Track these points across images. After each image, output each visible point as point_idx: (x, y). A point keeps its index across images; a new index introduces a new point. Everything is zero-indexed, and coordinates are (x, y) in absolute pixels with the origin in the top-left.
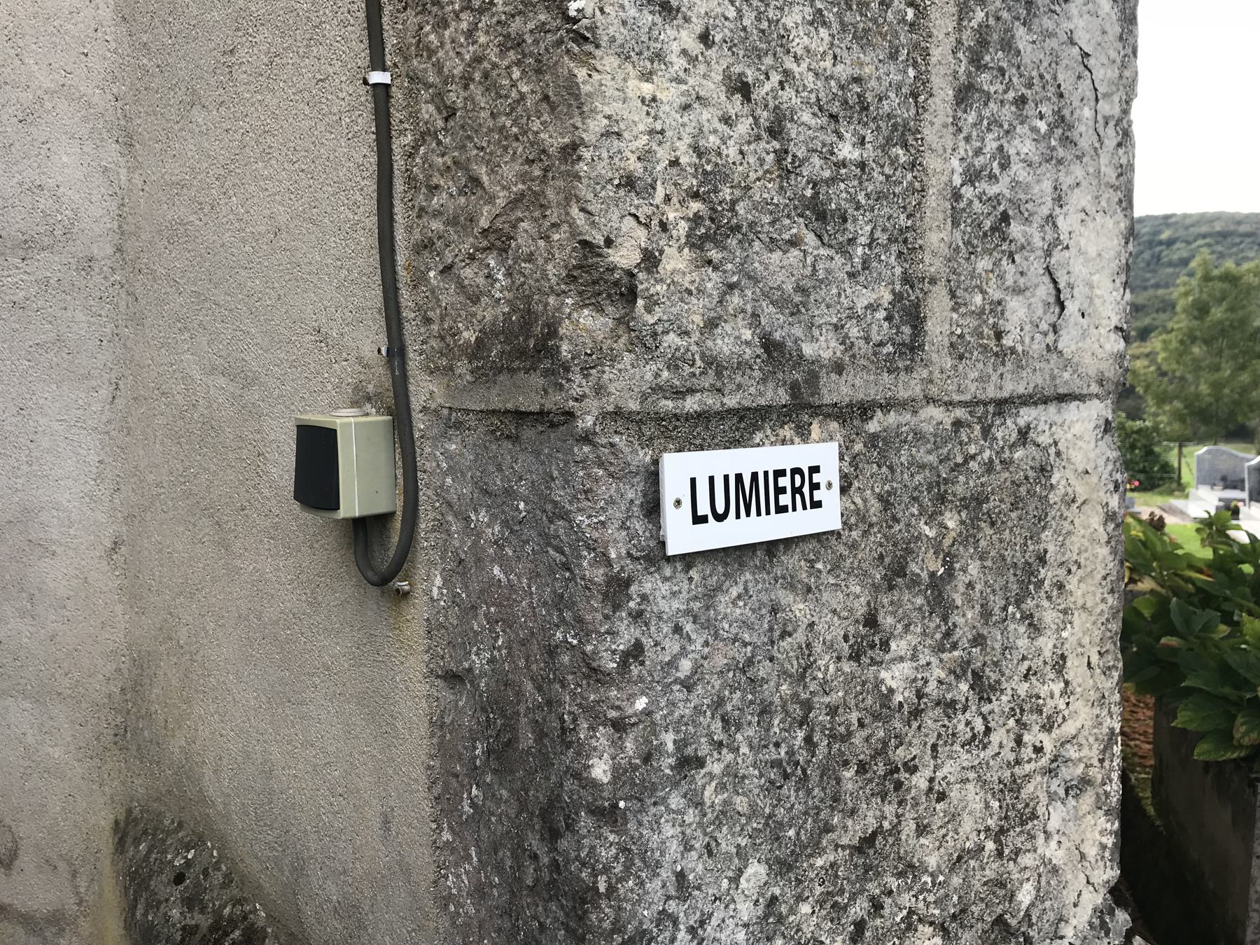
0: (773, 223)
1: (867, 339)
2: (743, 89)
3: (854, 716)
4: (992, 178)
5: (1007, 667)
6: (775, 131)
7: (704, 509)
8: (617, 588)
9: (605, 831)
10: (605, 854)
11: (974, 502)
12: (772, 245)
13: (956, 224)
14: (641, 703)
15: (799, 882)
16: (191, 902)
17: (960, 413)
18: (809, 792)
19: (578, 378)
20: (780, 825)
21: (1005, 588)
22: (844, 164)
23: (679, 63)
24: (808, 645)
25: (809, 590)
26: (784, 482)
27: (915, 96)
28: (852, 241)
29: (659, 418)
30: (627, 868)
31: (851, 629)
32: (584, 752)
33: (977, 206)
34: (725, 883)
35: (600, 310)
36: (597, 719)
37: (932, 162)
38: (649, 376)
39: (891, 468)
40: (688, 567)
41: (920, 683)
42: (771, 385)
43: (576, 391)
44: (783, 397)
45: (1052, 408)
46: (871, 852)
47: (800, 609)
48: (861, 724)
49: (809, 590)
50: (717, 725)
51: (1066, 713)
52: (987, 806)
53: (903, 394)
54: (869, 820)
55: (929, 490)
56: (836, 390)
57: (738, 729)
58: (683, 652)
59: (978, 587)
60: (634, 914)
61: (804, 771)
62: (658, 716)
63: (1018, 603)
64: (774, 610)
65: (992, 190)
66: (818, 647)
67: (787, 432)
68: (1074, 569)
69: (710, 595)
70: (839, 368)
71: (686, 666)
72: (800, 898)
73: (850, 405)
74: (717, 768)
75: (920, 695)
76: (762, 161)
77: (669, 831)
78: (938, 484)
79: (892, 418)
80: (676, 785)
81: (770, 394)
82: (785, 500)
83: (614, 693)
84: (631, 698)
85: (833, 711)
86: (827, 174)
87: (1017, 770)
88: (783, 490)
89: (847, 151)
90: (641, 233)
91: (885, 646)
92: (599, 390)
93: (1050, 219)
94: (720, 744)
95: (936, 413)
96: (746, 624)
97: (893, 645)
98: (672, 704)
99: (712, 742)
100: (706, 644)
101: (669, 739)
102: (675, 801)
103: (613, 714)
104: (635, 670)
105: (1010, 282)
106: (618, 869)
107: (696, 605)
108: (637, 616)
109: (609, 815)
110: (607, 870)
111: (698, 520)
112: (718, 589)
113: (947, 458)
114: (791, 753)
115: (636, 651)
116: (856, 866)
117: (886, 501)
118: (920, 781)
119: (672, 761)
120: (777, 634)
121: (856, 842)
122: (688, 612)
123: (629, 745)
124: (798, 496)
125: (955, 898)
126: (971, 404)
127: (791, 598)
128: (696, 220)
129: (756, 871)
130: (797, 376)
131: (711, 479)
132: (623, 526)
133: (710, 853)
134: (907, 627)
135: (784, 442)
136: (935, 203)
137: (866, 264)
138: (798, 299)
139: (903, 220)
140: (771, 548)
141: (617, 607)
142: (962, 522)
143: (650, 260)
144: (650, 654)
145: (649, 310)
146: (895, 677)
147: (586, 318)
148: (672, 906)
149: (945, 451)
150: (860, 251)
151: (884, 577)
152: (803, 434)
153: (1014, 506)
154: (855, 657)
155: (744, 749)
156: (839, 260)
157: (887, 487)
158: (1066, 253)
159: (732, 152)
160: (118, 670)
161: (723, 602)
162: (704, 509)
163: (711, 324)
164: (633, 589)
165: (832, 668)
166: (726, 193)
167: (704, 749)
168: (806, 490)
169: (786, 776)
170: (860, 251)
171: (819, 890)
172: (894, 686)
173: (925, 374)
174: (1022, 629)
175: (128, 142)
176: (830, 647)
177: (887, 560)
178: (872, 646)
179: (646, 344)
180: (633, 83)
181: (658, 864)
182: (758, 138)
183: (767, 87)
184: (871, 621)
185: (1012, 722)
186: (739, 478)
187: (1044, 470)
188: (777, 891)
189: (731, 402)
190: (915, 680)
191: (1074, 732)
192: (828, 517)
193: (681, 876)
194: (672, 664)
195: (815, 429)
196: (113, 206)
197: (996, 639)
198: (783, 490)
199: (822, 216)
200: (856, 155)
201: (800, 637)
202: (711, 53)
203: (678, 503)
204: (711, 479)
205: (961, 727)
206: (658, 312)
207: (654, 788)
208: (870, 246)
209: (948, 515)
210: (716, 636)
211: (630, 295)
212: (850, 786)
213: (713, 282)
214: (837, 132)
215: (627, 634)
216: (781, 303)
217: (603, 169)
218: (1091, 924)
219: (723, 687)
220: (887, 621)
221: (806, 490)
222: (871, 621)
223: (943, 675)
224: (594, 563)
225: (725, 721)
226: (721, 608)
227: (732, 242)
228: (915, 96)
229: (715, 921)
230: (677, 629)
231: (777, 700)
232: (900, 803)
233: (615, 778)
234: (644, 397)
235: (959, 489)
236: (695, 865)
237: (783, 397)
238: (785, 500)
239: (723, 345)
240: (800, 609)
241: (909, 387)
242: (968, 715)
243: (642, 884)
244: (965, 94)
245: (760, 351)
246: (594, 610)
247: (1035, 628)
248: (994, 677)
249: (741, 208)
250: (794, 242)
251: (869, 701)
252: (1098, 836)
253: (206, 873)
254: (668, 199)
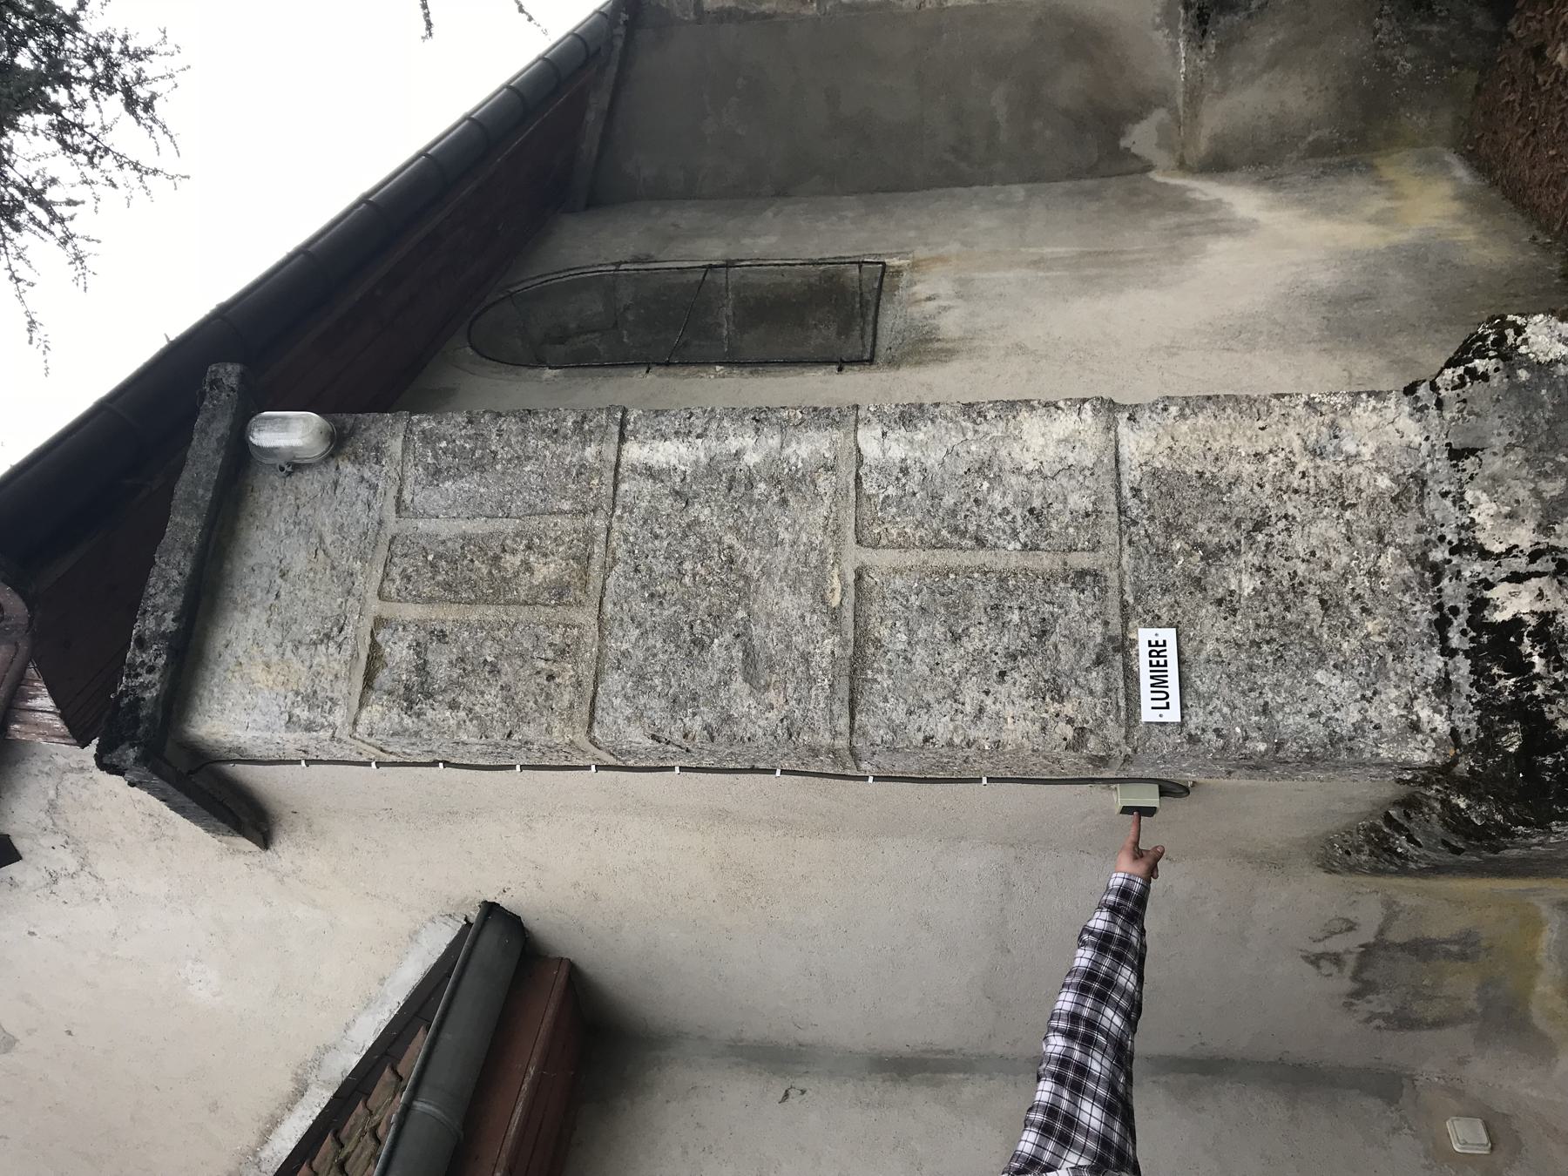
1: (1093, 604)
2: (1002, 674)
3: (1262, 614)
4: (1014, 520)
5: (1254, 502)
6: (1014, 657)
7: (1163, 704)
8: (1193, 739)
9: (1286, 747)
10: (1295, 747)
12: (1058, 659)
13: (1037, 548)
14: (1238, 730)
15: (1331, 650)
16: (1359, 851)
19: (1113, 752)
20: (1302, 660)
21: (1213, 502)
22: (1021, 619)
23: (998, 706)
24: (1226, 642)
25: (1201, 641)
26: (1154, 661)
27: (985, 573)
28: (1052, 614)
29: (1128, 718)
30: (1302, 739)
33: (1028, 531)
34: (1321, 692)
35: (1087, 740)
36: (1243, 746)
37: (1013, 565)
38: (1112, 724)
39: (1151, 586)
40: (1187, 706)
41: (1253, 570)
42: (1115, 664)
43: (1118, 753)
44: (1119, 657)
45: (1123, 468)
46: (1329, 602)
47: (1210, 647)
48: (1266, 610)
49: (1201, 641)
50: (1253, 695)
51: (1288, 450)
52: (1325, 518)
53: (1117, 584)
54: (1313, 604)
56: (1116, 629)
57: (1256, 683)
58: (1220, 711)
59: (1211, 525)
60: (1321, 739)
61: (1282, 646)
63: (1220, 492)
64: (1209, 661)
65: (1020, 521)
66: (1227, 637)
67: (1133, 653)
68: (1208, 446)
69: (1198, 695)
70: (1106, 623)
71: (1226, 710)
72: (1339, 650)
73: (1121, 617)
74: (1270, 695)
75: (1259, 569)
76: (1027, 665)
77: (1291, 721)
78: (1158, 555)
79: (1127, 588)
80: (1273, 716)
81: (1118, 664)
82: (1162, 663)
83: (1233, 740)
84: (1236, 734)
85: (1258, 626)
86: (1026, 628)
87: (1312, 492)
88: (1158, 662)
89: (1015, 617)
90: (1061, 724)
91: (1232, 593)
92: (1117, 745)
93: (1029, 475)
94: (1261, 693)
95: (1125, 558)
96: (1213, 678)
97: (1233, 588)
98: (1241, 716)
99: (1259, 697)
100: (1218, 699)
101: (1254, 719)
102: (1279, 717)
103: (1241, 741)
104: (1224, 732)
105: (1061, 506)
106: (1302, 742)
107: (1202, 704)
108: (1204, 730)
109: (1279, 746)
110: (1301, 747)
111: (1168, 707)
112: (1196, 692)
113: (1146, 548)
114: (1271, 654)
115: (1217, 731)
116: (1334, 612)
117: (1165, 591)
118: (1302, 568)
119: (1263, 718)
120: (1219, 659)
121: (1322, 612)
122: (1204, 708)
123: (1254, 735)
124: (1161, 654)
125: (1369, 542)
126: (1121, 533)
127: (1204, 652)
128: (1052, 699)
129: (1320, 676)
130: (1110, 649)
131: (1153, 699)
132: (1169, 736)
133: (1306, 699)
135: (1138, 655)
136: (1030, 561)
137: (1061, 607)
138: (1078, 645)
140: (1181, 662)
141: (1200, 741)
142: (1178, 538)
143: (1070, 721)
144: (1219, 726)
146: (1249, 585)
147: (1091, 745)
148: (1323, 719)
149: (1142, 550)
150: (1056, 610)
151: (1200, 592)
152: (1134, 643)
153: (1172, 495)
154: (1234, 611)
155: (1265, 680)
156: (1060, 621)
157: (1159, 590)
158: (1045, 463)
159: (1026, 681)
161: (1203, 689)
162: (1163, 704)
163: (1091, 693)
164: (1193, 732)
165: (1238, 627)
166: (1041, 684)
167: (1261, 701)
168: (1158, 649)
169: (1281, 657)
170: (1056, 610)
171: (1338, 638)
172: (1252, 587)
174: (1236, 492)
176: (1228, 628)
177: (1193, 589)
178: (1232, 601)
179: (1101, 724)
180: (1009, 727)
184: (1219, 602)
185: (1285, 497)
186: (1152, 685)
187: (1155, 474)
188: (1332, 663)
189: (1121, 684)
190: (1251, 573)
191: (1300, 441)
192: (1169, 635)
193: (1311, 715)
194: (1224, 716)
195: (1132, 636)
196: (989, 846)
197: (1239, 511)
198: (1158, 662)
199: (1044, 632)
200: (1016, 612)
201: (1221, 647)
202: (991, 689)
203: (1161, 716)
204: (1153, 699)
205: (1280, 538)
206: (1088, 718)
208: (1053, 604)
209: (1173, 548)
210: (1215, 693)
211: (1083, 729)
212: (1294, 616)
213: (1075, 691)
214: (1009, 623)
215: (1211, 735)
216: (1081, 654)
217: (1040, 740)
218: (1419, 421)
219: (1237, 690)
220: (1221, 592)
221: (1158, 649)
222: (1219, 602)
223: (1251, 553)
225: (1251, 690)
226: (1205, 690)
227: (1059, 681)
228: (985, 573)
230: (1211, 713)
231: (1247, 661)
232: (1310, 582)
233: (1266, 742)
234: (1120, 726)
235: (1160, 540)
236: (1310, 707)
237: (1119, 657)
238: (1162, 663)
239: (1099, 687)
241: (1113, 575)
242: (1275, 533)
243: (1310, 734)
244: (980, 542)
245: (1101, 666)
246: (1200, 748)
247: (1237, 480)
248: (1259, 512)
249: (1046, 677)
250: (1056, 647)
251: (1256, 603)
253: (1346, 841)
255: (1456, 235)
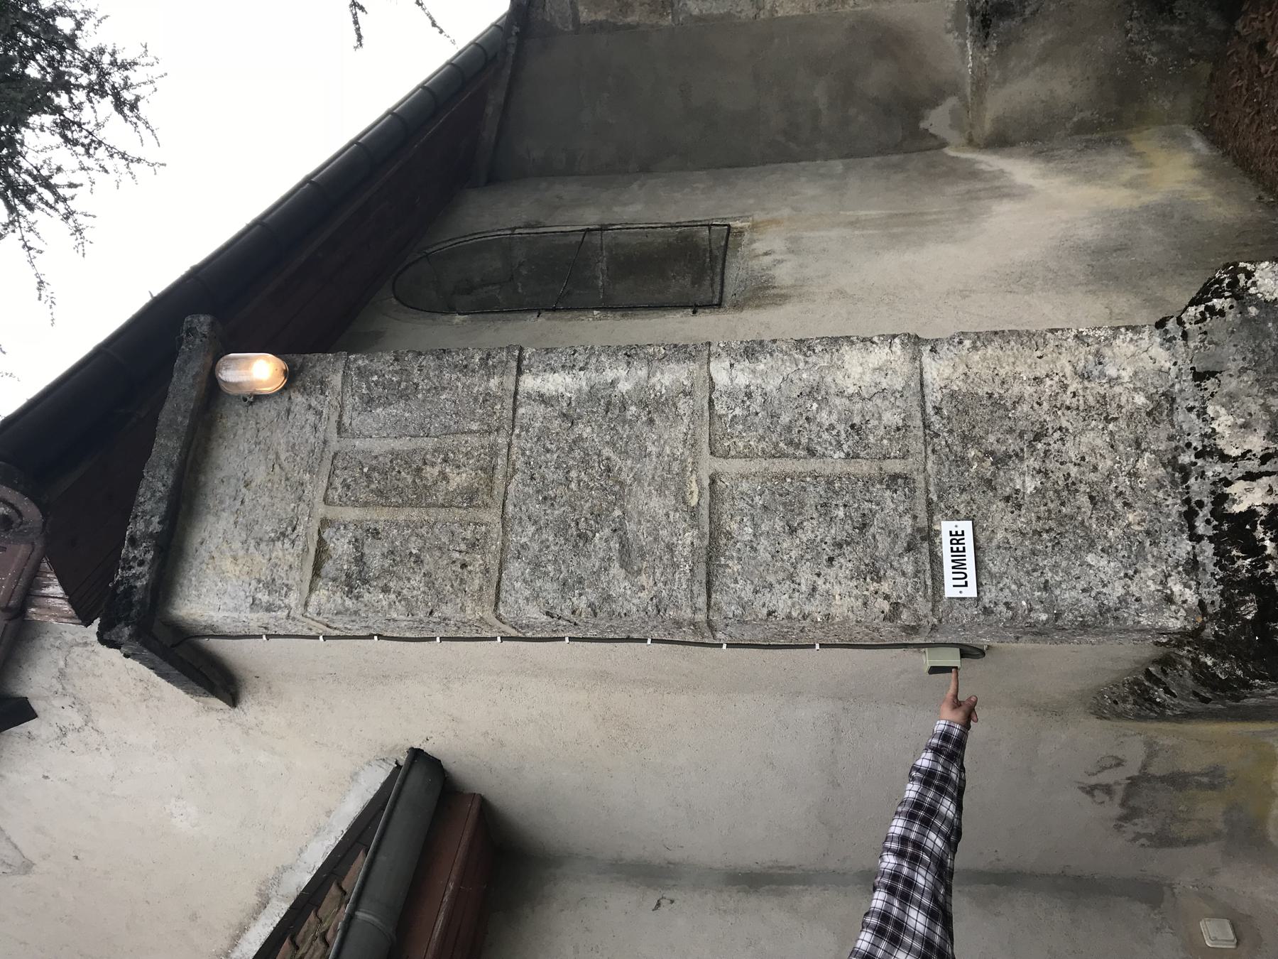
0: (869, 547)
1: (904, 502)
2: (831, 560)
3: (1042, 508)
4: (838, 434)
6: (840, 546)
7: (962, 582)
8: (987, 611)
9: (1063, 617)
10: (1071, 617)
11: (965, 438)
12: (876, 547)
13: (858, 457)
15: (1099, 538)
16: (1125, 701)
17: (929, 452)
18: (1067, 532)
19: (922, 622)
20: (1076, 545)
21: (1001, 418)
22: (845, 514)
24: (1013, 531)
26: (955, 548)
27: (816, 477)
29: (934, 594)
31: (1009, 509)
32: (1037, 621)
33: (850, 443)
34: (1091, 571)
35: (901, 612)
36: (1028, 616)
37: (838, 471)
38: (921, 599)
39: (951, 487)
40: (982, 584)
41: (1035, 472)
42: (922, 550)
43: (926, 623)
44: (926, 545)
45: (927, 391)
46: (1097, 498)
47: (1000, 535)
50: (1035, 574)
51: (1061, 374)
52: (1093, 429)
53: (923, 485)
54: (1084, 500)
55: (958, 466)
57: (1038, 565)
58: (1009, 588)
59: (999, 436)
60: (1092, 610)
61: (1058, 534)
62: (1029, 597)
64: (999, 547)
65: (843, 435)
66: (1014, 527)
67: (937, 541)
68: (996, 372)
69: (992, 575)
70: (915, 517)
71: (1014, 587)
72: (1105, 537)
74: (1050, 574)
75: (1039, 472)
76: (851, 552)
77: (1067, 596)
78: (957, 461)
79: (932, 489)
80: (1052, 592)
82: (961, 549)
83: (1020, 612)
84: (1022, 606)
85: (1039, 518)
86: (850, 522)
87: (1081, 408)
88: (958, 548)
89: (841, 513)
90: (879, 600)
91: (1017, 491)
92: (926, 616)
93: (850, 398)
94: (1042, 573)
95: (930, 464)
97: (1018, 487)
99: (1041, 576)
101: (1037, 594)
102: (1057, 592)
103: (1026, 612)
104: (1013, 605)
105: (876, 423)
106: (1077, 613)
108: (996, 604)
109: (1058, 616)
110: (1076, 617)
111: (966, 585)
112: (989, 572)
113: (947, 456)
114: (1050, 541)
115: (1007, 604)
117: (963, 490)
118: (1074, 471)
119: (1044, 593)
120: (1008, 546)
121: (1091, 506)
122: (996, 586)
123: (1037, 607)
124: (960, 542)
125: (1129, 449)
126: (926, 443)
128: (872, 579)
129: (1090, 558)
130: (918, 538)
131: (954, 579)
132: (967, 609)
133: (1079, 578)
134: (1011, 480)
135: (941, 543)
139: (860, 484)
140: (976, 548)
141: (992, 612)
143: (887, 597)
144: (1009, 600)
145: (901, 598)
146: (1031, 485)
147: (904, 616)
148: (1093, 594)
150: (874, 507)
152: (938, 533)
153: (967, 413)
154: (1019, 507)
155: (1045, 563)
156: (877, 516)
158: (863, 388)
159: (850, 565)
160: (1025, 712)
161: (995, 570)
162: (962, 582)
163: (904, 574)
164: (987, 606)
165: (1023, 520)
166: (863, 567)
167: (1042, 580)
168: (958, 538)
169: (1058, 543)
170: (874, 507)
171: (1105, 527)
172: (1033, 486)
173: (915, 473)
174: (1019, 409)
175: (799, 693)
179: (911, 599)
181: (1077, 600)
182: (844, 554)
183: (827, 549)
184: (1007, 499)
185: (1059, 413)
186: (953, 568)
187: (953, 395)
188: (1100, 548)
189: (928, 567)
190: (1033, 475)
191: (1071, 367)
192: (967, 526)
193: (1084, 590)
194: (1012, 592)
195: (936, 527)
197: (1022, 424)
198: (958, 548)
199: (864, 525)
200: (842, 508)
202: (822, 572)
203: (961, 592)
204: (954, 579)
205: (1056, 446)
206: (901, 595)
207: (1052, 601)
208: (872, 502)
210: (1005, 573)
211: (897, 604)
213: (890, 573)
215: (1002, 608)
216: (894, 543)
218: (1168, 349)
221: (958, 538)
222: (1007, 499)
223: (1033, 459)
224: (978, 618)
225: (1034, 570)
226: (996, 570)
227: (877, 565)
228: (816, 477)
229: (1103, 576)
231: (1030, 547)
232: (1081, 482)
233: (1047, 613)
234: (928, 601)
236: (1082, 584)
237: (926, 545)
238: (961, 549)
239: (910, 569)
240: (1000, 535)
241: (920, 478)
242: (1051, 442)
243: (1083, 606)
244: (811, 452)
246: (992, 618)
247: (1019, 400)
248: (1038, 426)
249: (867, 562)
250: (874, 537)
251: (1037, 499)
252: (1125, 345)
253: (1114, 693)
254: (867, 590)
255: (1140, 176)
